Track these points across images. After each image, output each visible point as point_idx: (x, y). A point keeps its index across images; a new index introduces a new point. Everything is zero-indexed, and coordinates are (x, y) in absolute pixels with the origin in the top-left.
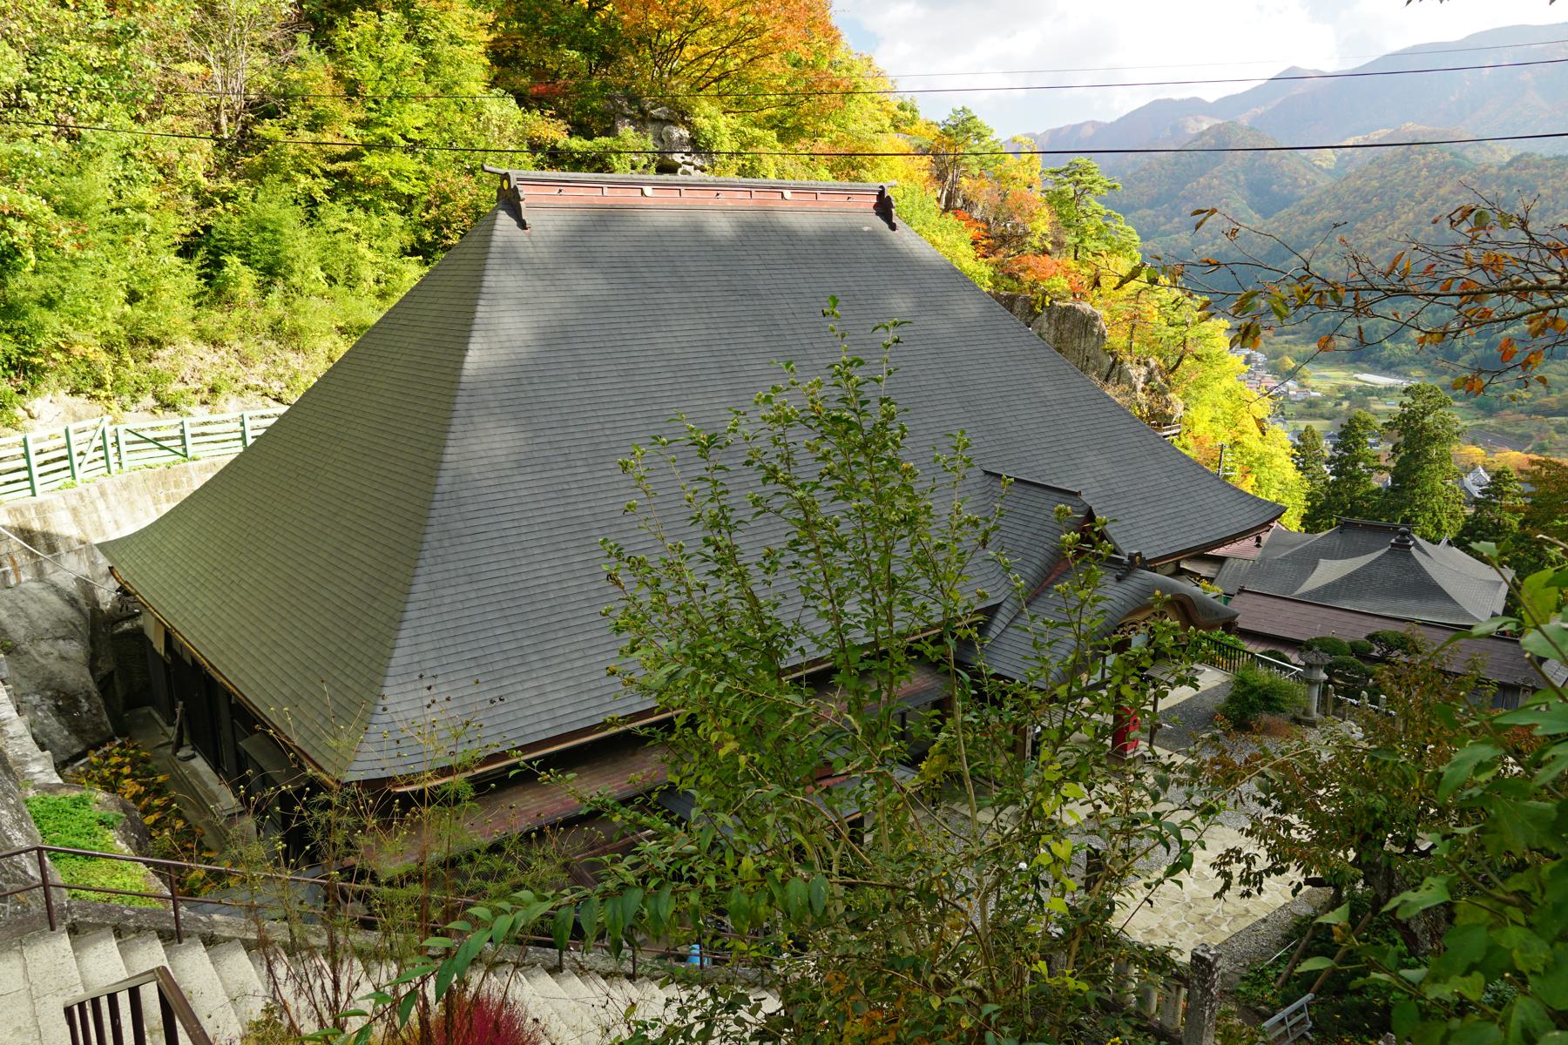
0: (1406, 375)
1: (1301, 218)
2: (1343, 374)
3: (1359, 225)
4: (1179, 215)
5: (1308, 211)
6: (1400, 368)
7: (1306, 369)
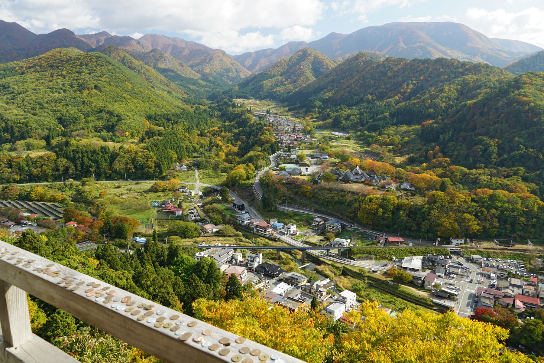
0: (348, 132)
2: (328, 132)
5: (327, 76)
6: (346, 130)
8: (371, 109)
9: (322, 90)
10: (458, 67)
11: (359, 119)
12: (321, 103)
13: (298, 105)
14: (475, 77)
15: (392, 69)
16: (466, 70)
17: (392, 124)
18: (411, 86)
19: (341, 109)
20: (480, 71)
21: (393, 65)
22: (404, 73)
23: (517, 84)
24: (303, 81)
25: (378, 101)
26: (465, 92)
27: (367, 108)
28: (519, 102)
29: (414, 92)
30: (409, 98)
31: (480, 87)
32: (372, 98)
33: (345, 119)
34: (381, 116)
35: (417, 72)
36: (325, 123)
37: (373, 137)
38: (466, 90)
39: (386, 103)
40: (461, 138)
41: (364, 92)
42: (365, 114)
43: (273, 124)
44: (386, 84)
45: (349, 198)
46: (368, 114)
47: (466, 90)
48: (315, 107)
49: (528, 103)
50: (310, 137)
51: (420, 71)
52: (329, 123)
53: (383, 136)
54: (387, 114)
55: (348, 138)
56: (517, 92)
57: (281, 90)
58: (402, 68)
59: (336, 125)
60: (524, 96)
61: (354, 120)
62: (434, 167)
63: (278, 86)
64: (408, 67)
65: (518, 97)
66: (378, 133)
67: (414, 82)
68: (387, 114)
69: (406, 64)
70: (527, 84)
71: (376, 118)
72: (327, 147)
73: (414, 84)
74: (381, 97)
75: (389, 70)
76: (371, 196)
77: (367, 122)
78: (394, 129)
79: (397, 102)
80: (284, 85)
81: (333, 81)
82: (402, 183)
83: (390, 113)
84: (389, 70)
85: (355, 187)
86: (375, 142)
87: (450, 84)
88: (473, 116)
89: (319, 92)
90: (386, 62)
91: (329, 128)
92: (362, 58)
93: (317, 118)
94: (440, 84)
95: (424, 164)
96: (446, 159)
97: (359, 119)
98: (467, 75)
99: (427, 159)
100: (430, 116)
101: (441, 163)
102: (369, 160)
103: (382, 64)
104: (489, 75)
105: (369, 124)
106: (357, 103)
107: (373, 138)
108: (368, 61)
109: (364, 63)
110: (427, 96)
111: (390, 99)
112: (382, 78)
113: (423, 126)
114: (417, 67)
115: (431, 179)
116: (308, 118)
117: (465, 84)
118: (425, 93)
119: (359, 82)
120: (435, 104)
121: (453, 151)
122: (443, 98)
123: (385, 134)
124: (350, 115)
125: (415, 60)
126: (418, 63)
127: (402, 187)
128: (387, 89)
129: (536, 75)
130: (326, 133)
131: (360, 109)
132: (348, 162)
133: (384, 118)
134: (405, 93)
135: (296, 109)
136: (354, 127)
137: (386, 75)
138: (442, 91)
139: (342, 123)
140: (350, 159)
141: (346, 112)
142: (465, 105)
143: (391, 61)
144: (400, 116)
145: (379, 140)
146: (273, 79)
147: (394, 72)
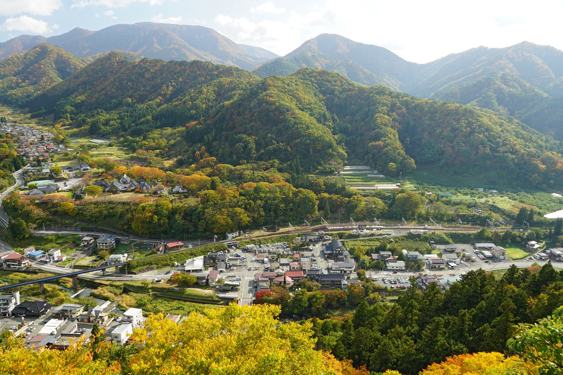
1: (74, 80)
2: (86, 140)
3: (95, 83)
4: (28, 79)
5: (76, 77)
6: (107, 136)
7: (68, 139)
8: (131, 112)
9: (73, 93)
10: (213, 70)
11: (120, 123)
12: (73, 108)
13: (44, 111)
14: (229, 80)
15: (149, 70)
16: (221, 73)
17: (156, 128)
18: (171, 88)
19: (98, 114)
20: (232, 74)
21: (149, 66)
22: (162, 74)
23: (264, 86)
24: (46, 82)
25: (139, 104)
26: (222, 93)
27: (127, 112)
28: (267, 102)
29: (175, 94)
30: (168, 100)
31: (234, 89)
32: (132, 100)
33: (103, 125)
34: (143, 119)
35: (175, 74)
36: (81, 130)
37: (137, 142)
38: (223, 91)
39: (148, 105)
40: (223, 137)
41: (123, 95)
42: (126, 119)
43: (11, 135)
44: (144, 86)
45: (120, 209)
46: (129, 118)
47: (223, 91)
48: (66, 112)
49: (274, 103)
50: (64, 147)
51: (178, 73)
52: (86, 129)
53: (149, 140)
54: (149, 117)
55: (110, 145)
56: (264, 93)
57: (18, 92)
58: (160, 70)
59: (94, 132)
60: (271, 97)
61: (114, 125)
62: (203, 167)
63: (12, 88)
64: (166, 69)
65: (266, 97)
66: (142, 137)
67: (173, 83)
68: (149, 117)
69: (163, 66)
70: (271, 86)
71: (138, 122)
72: (87, 157)
73: (173, 86)
74: (141, 100)
75: (146, 71)
76: (143, 204)
77: (130, 127)
78: (159, 133)
79: (159, 105)
80: (21, 87)
81: (84, 83)
82: (173, 187)
83: (153, 116)
84: (146, 71)
85: (125, 197)
86: (141, 147)
87: (207, 86)
88: (232, 116)
89: (68, 96)
90: (142, 63)
91: (87, 135)
92: (115, 58)
93: (70, 125)
94: (199, 86)
95: (193, 165)
96: (213, 158)
97: (120, 123)
98: (222, 77)
99: (195, 160)
100: (192, 118)
101: (208, 162)
102: (137, 167)
103: (138, 65)
104: (240, 78)
105: (132, 129)
106: (116, 107)
107: (137, 144)
108: (122, 62)
109: (118, 63)
110: (187, 97)
111: (151, 102)
112: (140, 80)
113: (187, 128)
114: (175, 69)
115: (201, 179)
116: (58, 126)
117: (221, 86)
118: (185, 95)
119: (115, 84)
120: (196, 106)
121: (218, 150)
122: (202, 99)
123: (150, 138)
124: (110, 120)
125: (171, 62)
126: (175, 65)
127: (174, 190)
128: (147, 91)
129: (277, 78)
130: (83, 141)
131: (120, 113)
132: (114, 170)
133: (147, 122)
134: (165, 95)
135: (42, 116)
136: (115, 132)
137: (143, 77)
138: (201, 92)
139: (101, 129)
140: (116, 167)
141: (104, 116)
142: (223, 106)
143: (147, 62)
144: (163, 119)
145: (145, 144)
146: (4, 79)
147: (152, 73)
